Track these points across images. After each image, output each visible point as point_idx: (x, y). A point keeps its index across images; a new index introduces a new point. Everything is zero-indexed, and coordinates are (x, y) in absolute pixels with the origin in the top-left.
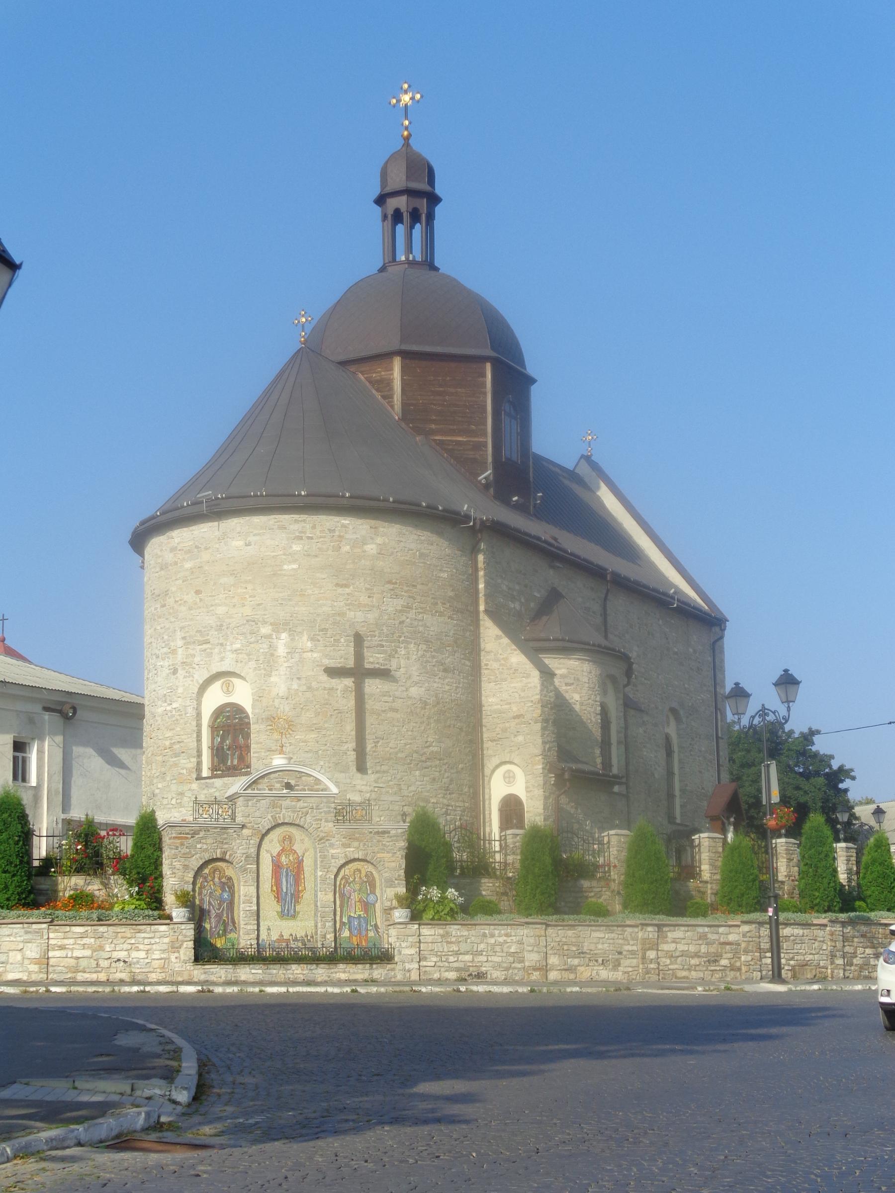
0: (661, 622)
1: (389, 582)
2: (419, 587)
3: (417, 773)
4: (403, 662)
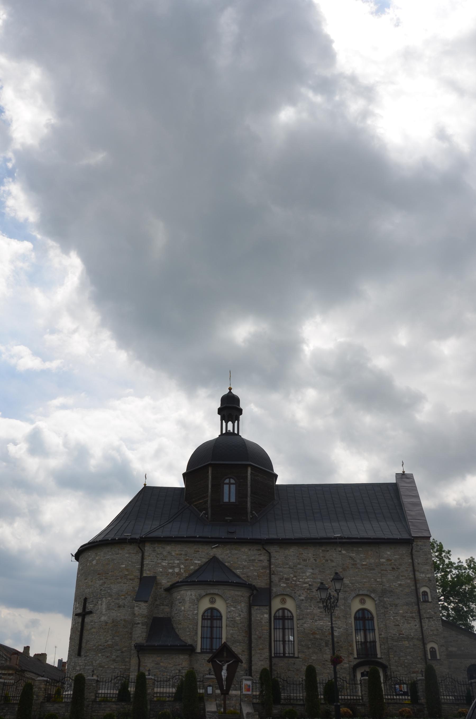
0: (344, 552)
1: (99, 574)
2: (110, 573)
3: (100, 655)
4: (100, 607)
